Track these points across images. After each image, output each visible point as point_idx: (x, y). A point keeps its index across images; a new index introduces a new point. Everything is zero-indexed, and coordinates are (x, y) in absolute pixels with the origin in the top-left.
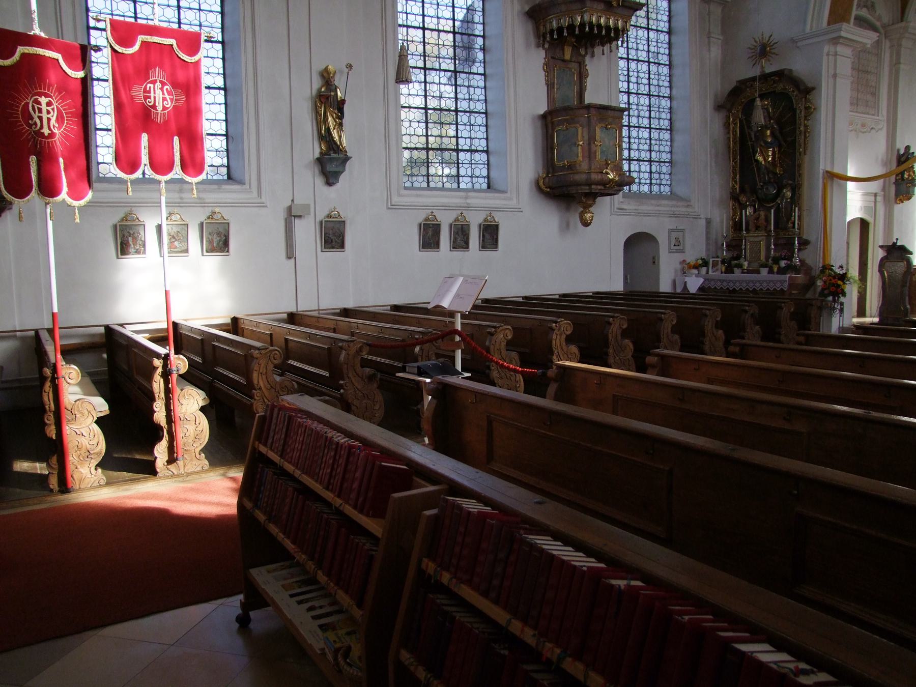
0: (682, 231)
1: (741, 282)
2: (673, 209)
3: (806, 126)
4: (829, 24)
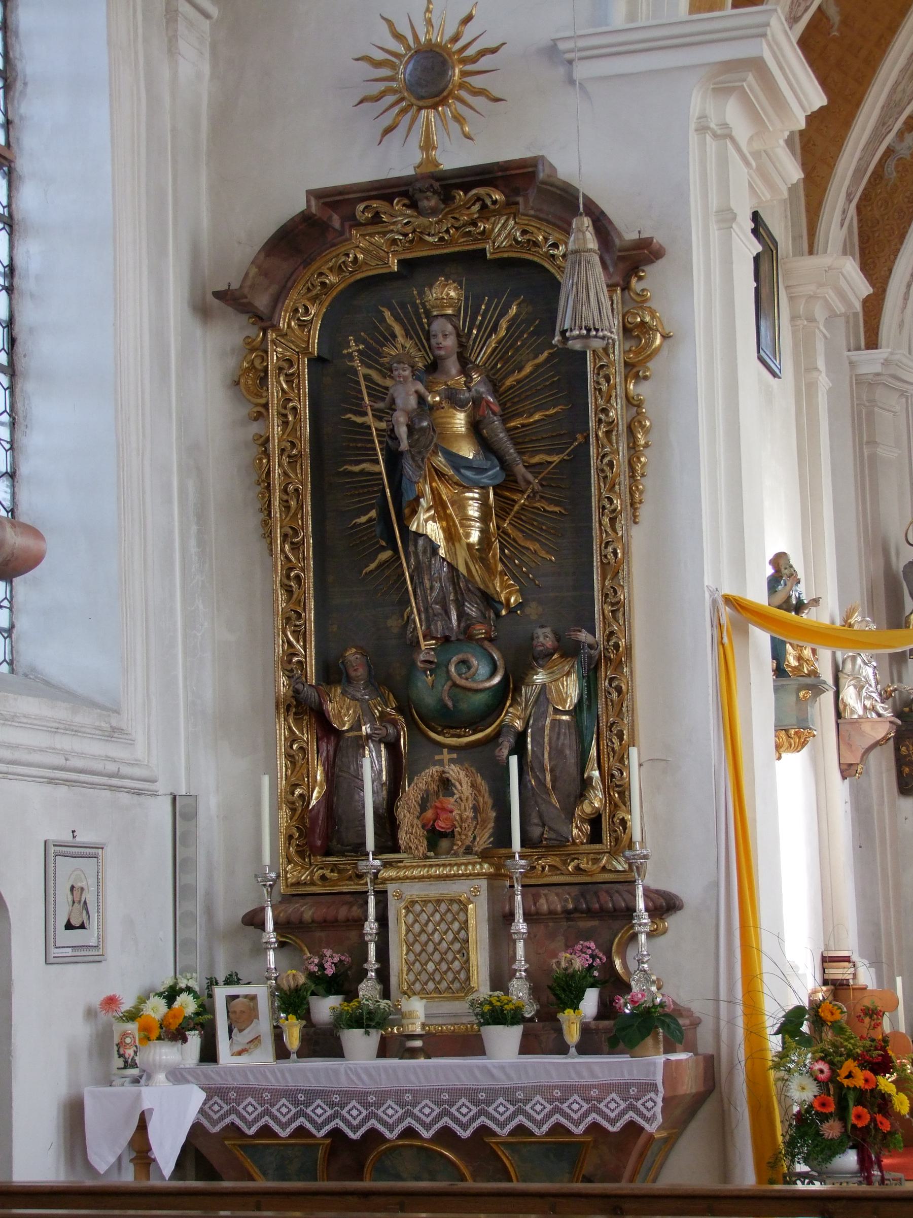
0: (91, 852)
1: (371, 1101)
2: (65, 742)
3: (632, 403)
4: (691, 12)
